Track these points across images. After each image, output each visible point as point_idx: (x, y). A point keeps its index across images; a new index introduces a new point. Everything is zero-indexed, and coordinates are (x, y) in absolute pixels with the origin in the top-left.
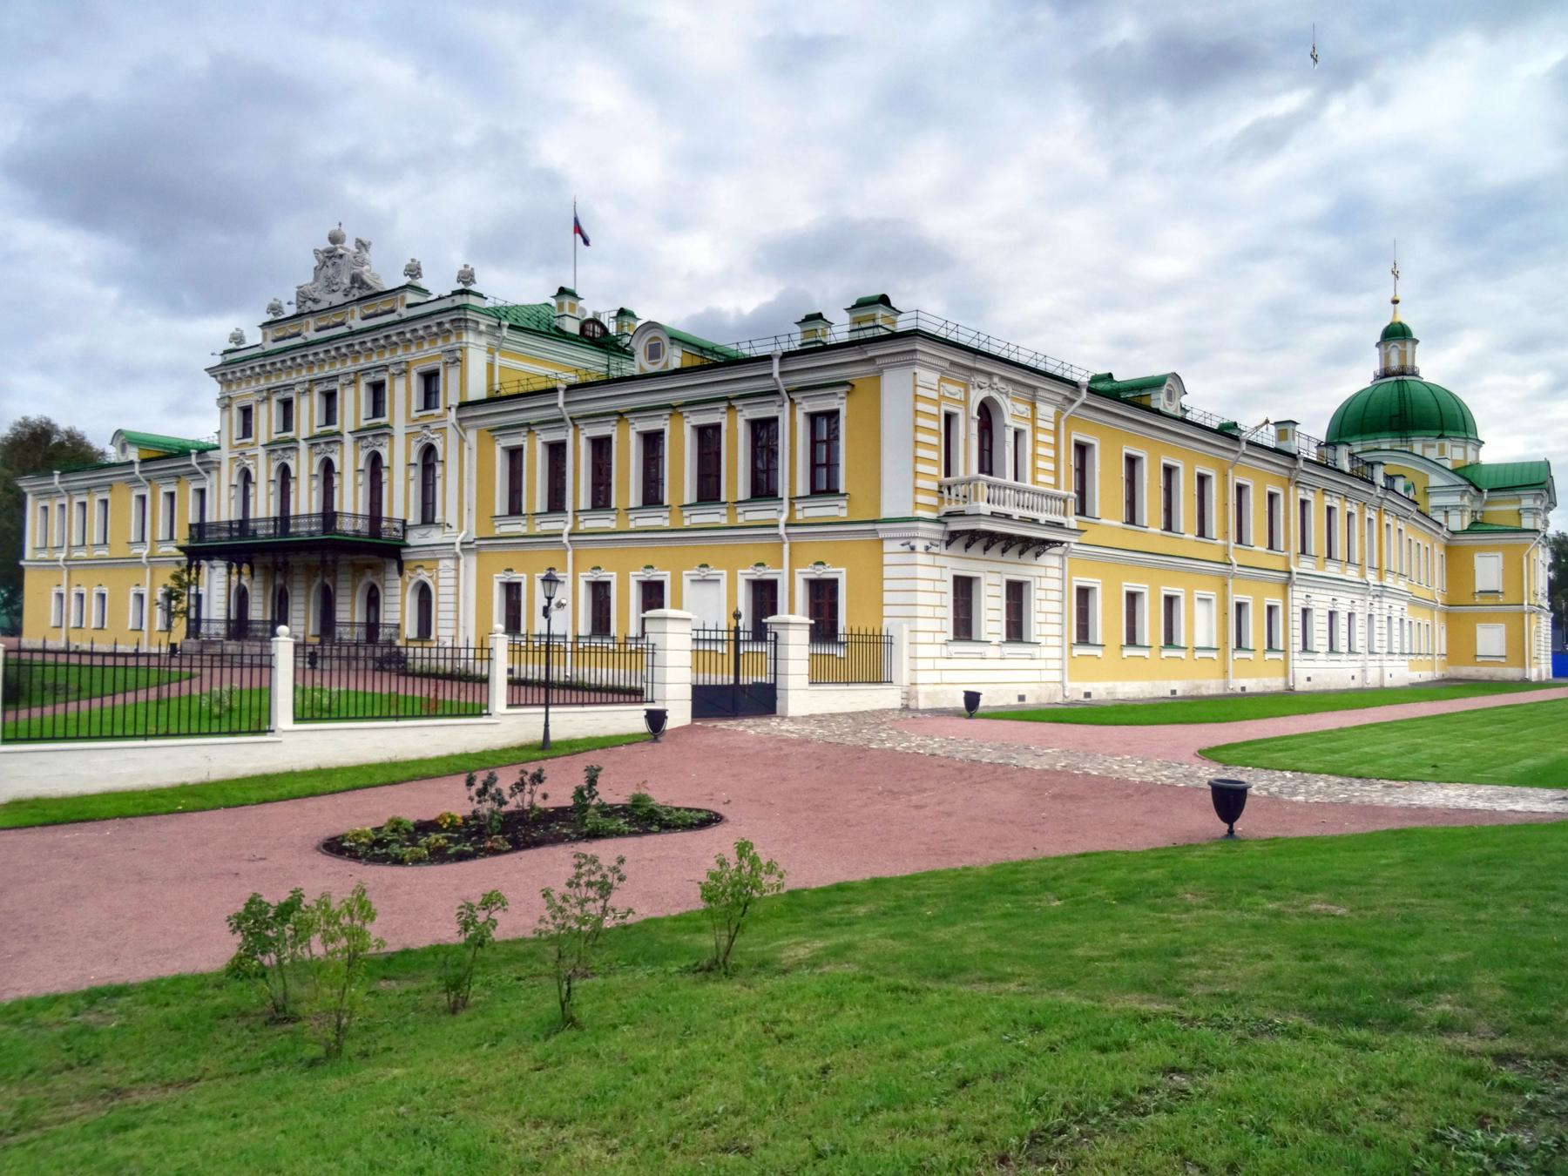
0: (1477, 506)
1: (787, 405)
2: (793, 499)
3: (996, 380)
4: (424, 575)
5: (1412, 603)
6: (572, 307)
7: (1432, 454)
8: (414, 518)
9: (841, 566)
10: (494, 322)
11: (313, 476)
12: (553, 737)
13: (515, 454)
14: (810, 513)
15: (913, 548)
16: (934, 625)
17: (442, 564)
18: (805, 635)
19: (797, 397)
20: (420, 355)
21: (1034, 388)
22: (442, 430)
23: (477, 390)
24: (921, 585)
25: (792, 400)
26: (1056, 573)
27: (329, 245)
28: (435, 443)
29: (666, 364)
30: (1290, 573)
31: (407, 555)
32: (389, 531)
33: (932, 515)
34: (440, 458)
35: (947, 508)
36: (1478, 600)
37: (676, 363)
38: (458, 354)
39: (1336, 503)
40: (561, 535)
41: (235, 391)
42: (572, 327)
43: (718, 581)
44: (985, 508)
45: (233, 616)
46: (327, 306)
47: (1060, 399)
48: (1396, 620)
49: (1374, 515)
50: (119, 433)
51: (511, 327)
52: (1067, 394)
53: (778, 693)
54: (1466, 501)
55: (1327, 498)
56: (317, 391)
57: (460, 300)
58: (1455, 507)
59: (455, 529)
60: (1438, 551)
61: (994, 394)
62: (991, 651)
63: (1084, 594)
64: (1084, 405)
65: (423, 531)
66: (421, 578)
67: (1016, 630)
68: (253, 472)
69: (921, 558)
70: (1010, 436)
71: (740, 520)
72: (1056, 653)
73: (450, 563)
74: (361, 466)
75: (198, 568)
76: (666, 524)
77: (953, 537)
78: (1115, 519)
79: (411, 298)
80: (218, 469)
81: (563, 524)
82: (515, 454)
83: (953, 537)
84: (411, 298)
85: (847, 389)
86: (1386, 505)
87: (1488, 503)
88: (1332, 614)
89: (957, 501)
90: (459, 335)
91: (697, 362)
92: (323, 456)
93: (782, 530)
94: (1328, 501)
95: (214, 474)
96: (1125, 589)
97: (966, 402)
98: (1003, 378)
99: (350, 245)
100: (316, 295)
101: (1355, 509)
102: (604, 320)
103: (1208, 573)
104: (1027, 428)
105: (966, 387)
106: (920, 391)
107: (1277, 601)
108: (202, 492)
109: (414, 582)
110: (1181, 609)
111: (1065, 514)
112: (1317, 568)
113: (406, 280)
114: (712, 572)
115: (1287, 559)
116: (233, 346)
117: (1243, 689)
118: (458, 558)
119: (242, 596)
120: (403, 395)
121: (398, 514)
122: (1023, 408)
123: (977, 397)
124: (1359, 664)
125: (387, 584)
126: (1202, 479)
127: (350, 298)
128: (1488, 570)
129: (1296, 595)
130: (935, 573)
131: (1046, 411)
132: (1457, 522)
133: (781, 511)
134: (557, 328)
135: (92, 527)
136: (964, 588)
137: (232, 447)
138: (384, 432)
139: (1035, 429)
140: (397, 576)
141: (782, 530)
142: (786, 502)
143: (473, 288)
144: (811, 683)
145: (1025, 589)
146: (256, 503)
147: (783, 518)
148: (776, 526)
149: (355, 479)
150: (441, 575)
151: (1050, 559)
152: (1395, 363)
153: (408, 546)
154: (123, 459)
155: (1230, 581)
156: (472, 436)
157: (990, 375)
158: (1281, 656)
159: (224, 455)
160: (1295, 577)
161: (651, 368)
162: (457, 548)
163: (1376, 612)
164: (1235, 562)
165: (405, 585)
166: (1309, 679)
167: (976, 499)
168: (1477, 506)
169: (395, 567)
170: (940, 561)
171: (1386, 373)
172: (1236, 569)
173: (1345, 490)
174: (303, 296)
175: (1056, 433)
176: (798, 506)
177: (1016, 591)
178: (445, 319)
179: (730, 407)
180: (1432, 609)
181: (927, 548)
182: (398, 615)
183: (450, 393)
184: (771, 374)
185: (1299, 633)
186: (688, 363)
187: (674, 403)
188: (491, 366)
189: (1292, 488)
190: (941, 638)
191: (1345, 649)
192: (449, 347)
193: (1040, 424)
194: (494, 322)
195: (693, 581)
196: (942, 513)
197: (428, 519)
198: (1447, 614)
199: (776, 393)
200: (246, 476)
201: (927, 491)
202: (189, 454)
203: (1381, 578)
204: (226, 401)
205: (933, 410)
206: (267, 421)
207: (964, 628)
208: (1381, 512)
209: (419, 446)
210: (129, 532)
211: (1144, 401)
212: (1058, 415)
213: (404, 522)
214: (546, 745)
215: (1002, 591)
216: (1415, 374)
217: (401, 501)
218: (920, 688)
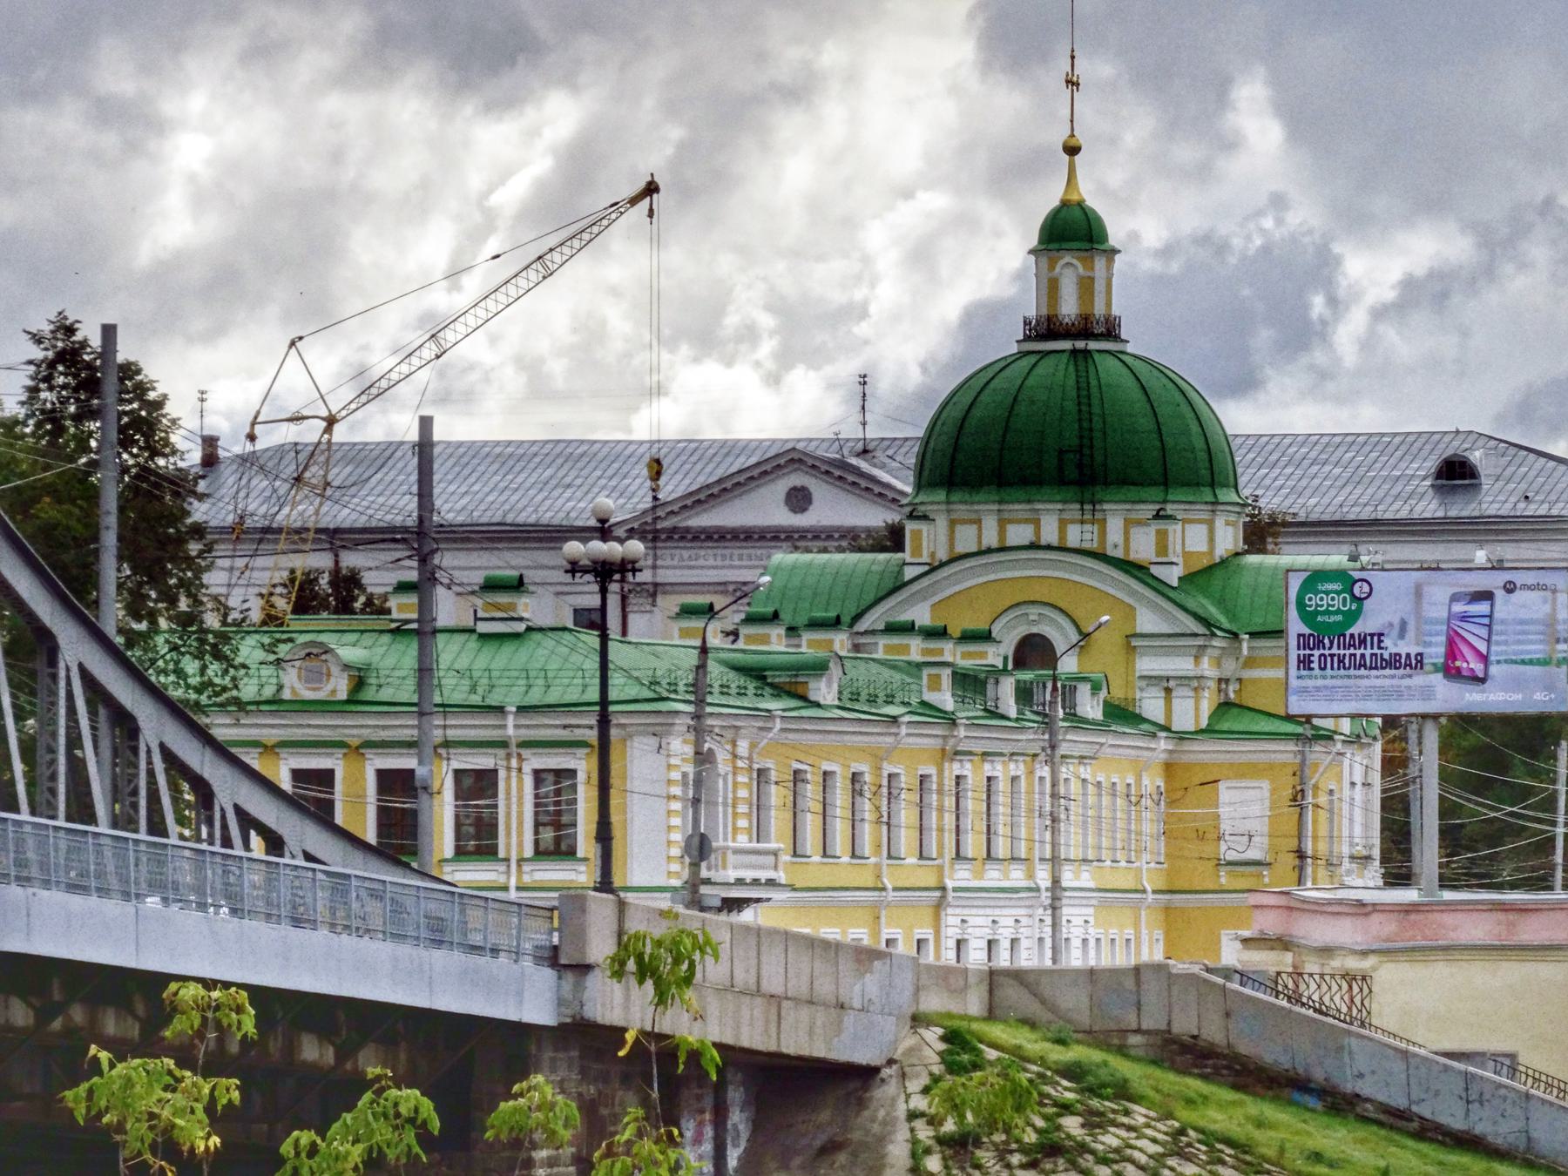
0: (1230, 667)
2: (521, 861)
7: (1143, 546)
14: (539, 876)
19: (525, 753)
25: (519, 755)
30: (944, 889)
54: (1207, 667)
58: (1184, 680)
87: (1250, 663)
103: (858, 904)
107: (927, 932)
115: (941, 868)
132: (1190, 712)
147: (513, 882)
148: (505, 889)
152: (1069, 308)
155: (884, 913)
160: (951, 894)
164: (889, 886)
168: (1230, 667)
171: (1046, 329)
176: (526, 868)
180: (1136, 907)
184: (504, 727)
198: (1167, 909)
216: (1111, 331)
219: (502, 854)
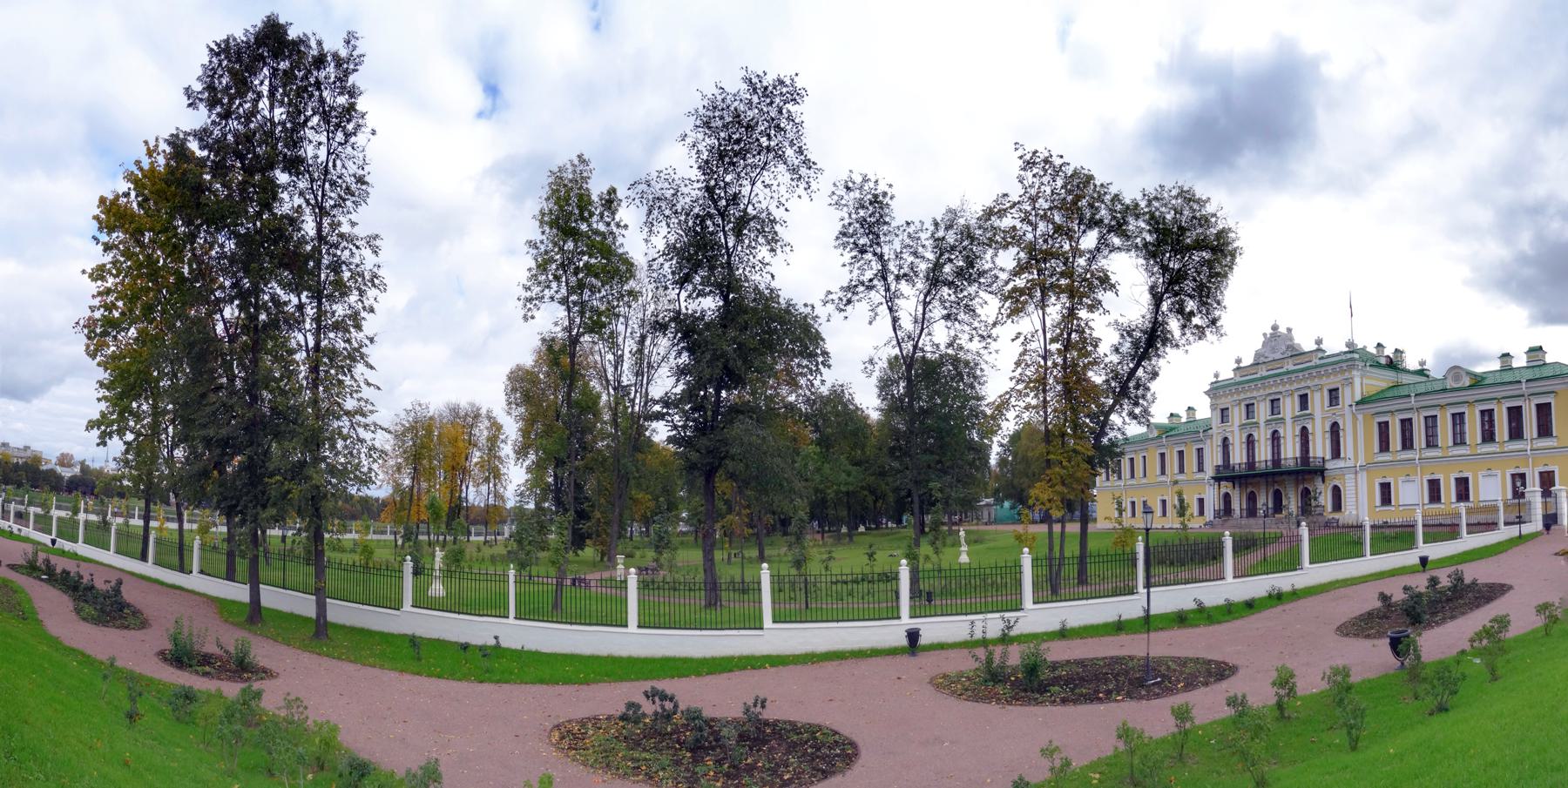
2: (1532, 439)
4: (1337, 483)
8: (1328, 456)
17: (1347, 477)
20: (1329, 381)
23: (1358, 397)
31: (1326, 473)
32: (1314, 464)
37: (1468, 384)
57: (1349, 356)
65: (1335, 461)
68: (1230, 438)
71: (1506, 449)
73: (1353, 476)
76: (1469, 452)
79: (1320, 355)
84: (1320, 355)
90: (1350, 372)
93: (1529, 452)
95: (1209, 441)
99: (1282, 330)
100: (1266, 355)
108: (1200, 451)
113: (1315, 347)
114: (1494, 472)
116: (1215, 380)
118: (1356, 473)
119: (1227, 497)
121: (1319, 454)
141: (1529, 452)
147: (1529, 448)
149: (1294, 439)
156: (1360, 417)
159: (1214, 431)
161: (1456, 386)
169: (1320, 479)
174: (1258, 355)
176: (1534, 442)
178: (1344, 365)
183: (1348, 397)
188: (1362, 384)
197: (1336, 453)
206: (1237, 416)
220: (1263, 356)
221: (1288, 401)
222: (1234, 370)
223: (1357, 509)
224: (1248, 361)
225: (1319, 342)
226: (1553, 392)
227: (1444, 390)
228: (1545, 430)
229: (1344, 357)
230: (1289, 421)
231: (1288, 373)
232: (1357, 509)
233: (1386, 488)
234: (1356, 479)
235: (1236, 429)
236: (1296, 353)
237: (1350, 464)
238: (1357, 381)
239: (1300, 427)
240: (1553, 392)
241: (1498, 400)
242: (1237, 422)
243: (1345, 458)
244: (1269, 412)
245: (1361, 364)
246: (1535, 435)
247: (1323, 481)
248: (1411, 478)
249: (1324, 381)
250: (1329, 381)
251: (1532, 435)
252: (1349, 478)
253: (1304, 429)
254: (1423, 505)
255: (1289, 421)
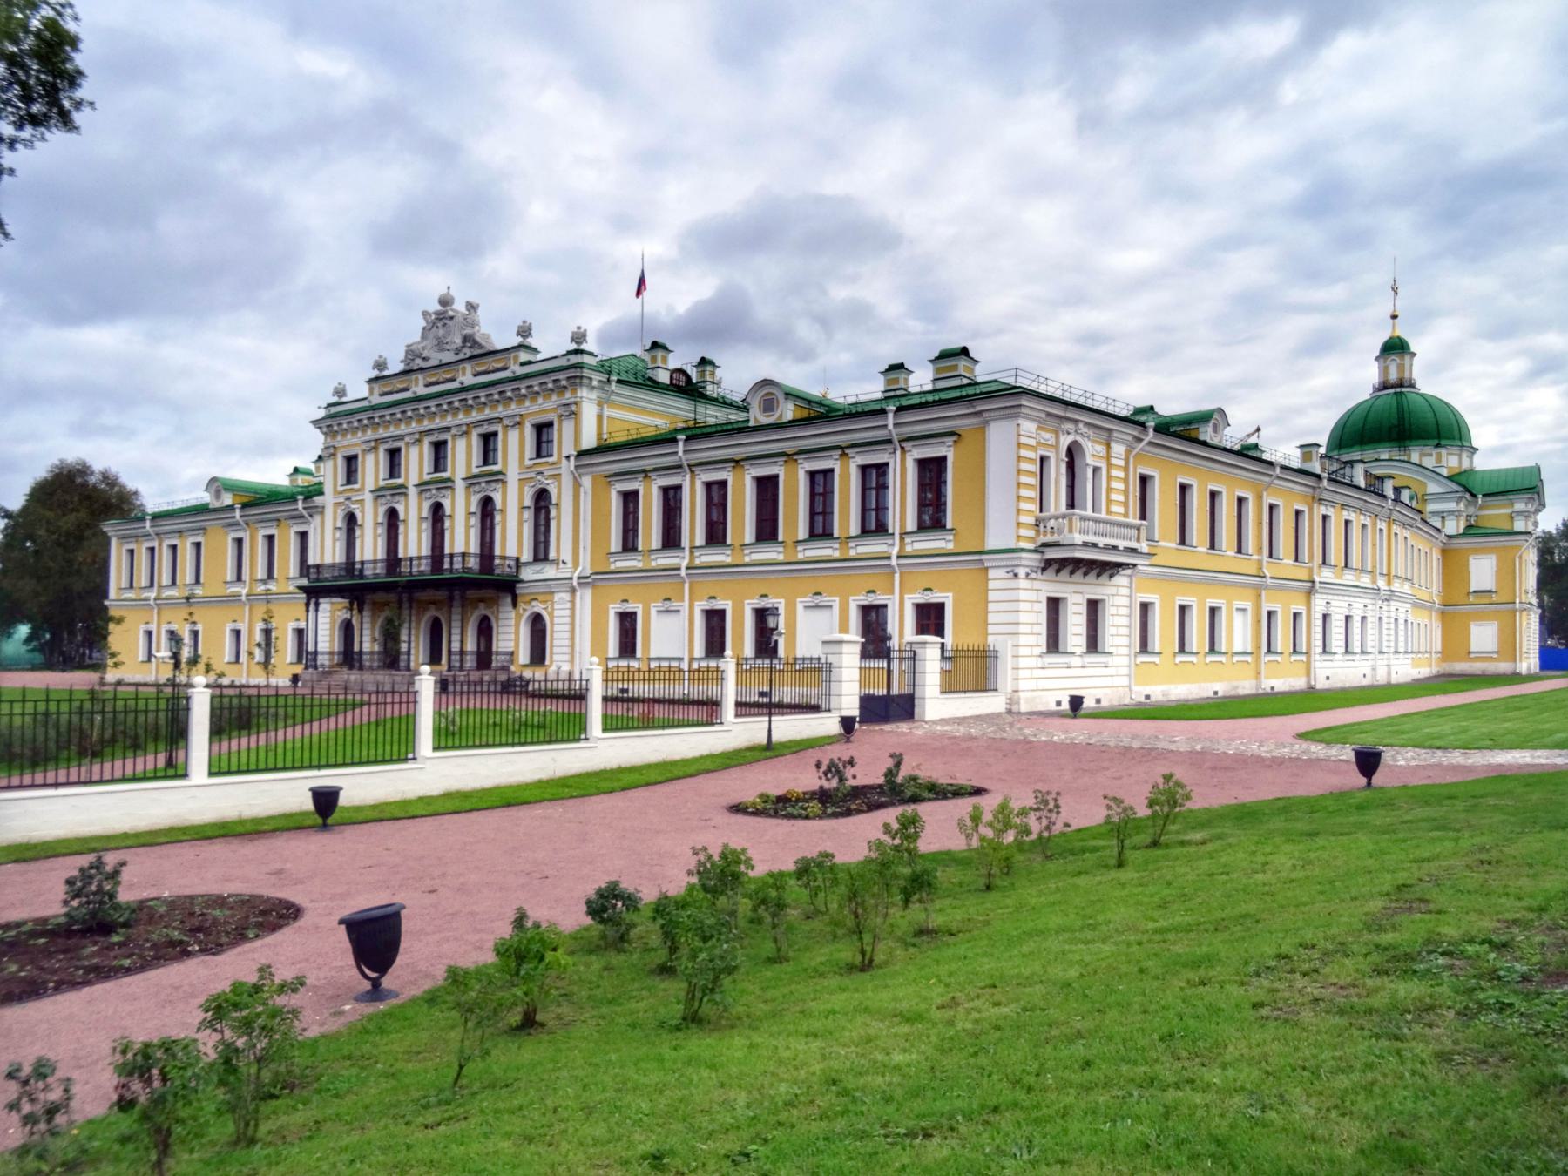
1: (898, 453)
2: (903, 535)
3: (1081, 425)
4: (538, 607)
5: (1415, 605)
6: (665, 360)
8: (526, 556)
9: (948, 591)
10: (604, 377)
11: (422, 519)
12: (775, 738)
13: (630, 498)
14: (918, 546)
15: (1016, 575)
16: (1032, 640)
17: (557, 597)
18: (857, 649)
19: (907, 445)
20: (535, 408)
21: (1110, 431)
22: (557, 477)
23: (589, 440)
24: (1023, 606)
25: (902, 448)
26: (1125, 591)
27: (439, 308)
28: (548, 488)
29: (781, 415)
30: (1313, 582)
31: (521, 589)
32: (502, 568)
33: (1031, 546)
34: (554, 501)
35: (1042, 539)
36: (1472, 599)
37: (789, 416)
38: (574, 408)
39: (1352, 516)
40: (679, 569)
41: (339, 441)
42: (663, 377)
43: (831, 607)
44: (1079, 538)
45: (482, 649)
46: (436, 363)
47: (1130, 438)
48: (1401, 621)
49: (1384, 525)
50: (214, 480)
51: (619, 381)
52: (1135, 433)
53: (916, 701)
55: (1345, 513)
56: (426, 441)
57: (574, 359)
59: (570, 565)
60: (1436, 555)
61: (1079, 438)
62: (1075, 661)
63: (1145, 607)
64: (1151, 443)
65: (538, 567)
66: (536, 609)
67: (1093, 644)
69: (1023, 583)
70: (1090, 472)
71: (852, 553)
72: (1125, 661)
73: (567, 596)
74: (473, 509)
75: (317, 605)
76: (781, 558)
77: (1048, 564)
78: (1170, 541)
79: (524, 356)
80: (322, 513)
81: (679, 559)
82: (630, 498)
83: (1048, 564)
84: (524, 356)
85: (955, 438)
86: (1395, 515)
88: (1347, 618)
89: (1045, 533)
90: (574, 392)
91: (805, 414)
92: (433, 501)
93: (894, 562)
94: (1346, 515)
95: (317, 518)
96: (1208, 605)
97: (1056, 447)
98: (1087, 424)
99: (459, 306)
101: (1368, 521)
102: (684, 368)
103: (1243, 585)
104: (1103, 466)
105: (1056, 433)
106: (1023, 440)
107: (1301, 608)
108: (303, 536)
109: (527, 614)
110: (1223, 618)
111: (1138, 540)
112: (1336, 577)
113: (517, 340)
114: (825, 600)
115: (1311, 570)
116: (335, 399)
117: (1272, 688)
118: (573, 591)
119: (347, 629)
120: (515, 448)
121: (512, 551)
122: (1100, 449)
123: (1065, 441)
124: (1370, 663)
125: (501, 616)
126: (1241, 501)
127: (461, 356)
128: (1482, 571)
129: (1318, 602)
130: (1032, 596)
131: (1118, 449)
132: (1453, 526)
133: (893, 545)
134: (650, 379)
135: (140, 564)
136: (1054, 605)
137: (336, 493)
138: (498, 478)
139: (1110, 466)
140: (510, 608)
141: (894, 562)
142: (897, 537)
143: (584, 347)
144: (943, 692)
145: (1100, 606)
146: (362, 542)
147: (895, 551)
148: (889, 558)
149: (467, 520)
150: (556, 606)
151: (1121, 580)
153: (522, 581)
154: (217, 504)
155: (1264, 593)
156: (587, 482)
157: (1076, 421)
158: (1303, 658)
159: (328, 500)
160: (1318, 585)
162: (575, 582)
163: (1384, 615)
165: (519, 617)
166: (1328, 678)
167: (1071, 531)
169: (509, 600)
170: (1037, 585)
172: (1269, 581)
173: (1360, 504)
174: (412, 354)
175: (1126, 469)
176: (908, 540)
177: (1094, 606)
178: (562, 376)
179: (844, 455)
180: (1430, 609)
181: (1027, 575)
182: (512, 644)
183: (565, 442)
184: (886, 426)
185: (1320, 636)
186: (798, 416)
187: (790, 451)
188: (600, 417)
189: (1315, 505)
190: (1037, 651)
191: (1358, 650)
192: (564, 401)
193: (1114, 461)
194: (604, 377)
195: (806, 607)
196: (1039, 544)
198: (1443, 613)
199: (889, 441)
200: (351, 519)
201: (1027, 525)
202: (296, 500)
203: (1389, 583)
204: (332, 451)
205: (1031, 455)
206: (373, 470)
207: (1054, 644)
208: (1390, 521)
209: (532, 491)
210: (226, 574)
211: (1193, 434)
212: (1128, 453)
213: (517, 559)
214: (769, 746)
215: (1083, 609)
217: (513, 539)
218: (1021, 694)
219: (890, 531)
220: (419, 356)
221: (461, 444)
222: (371, 381)
223: (572, 661)
224: (395, 366)
225: (525, 331)
226: (952, 434)
227: (741, 429)
228: (932, 516)
229: (563, 362)
230: (460, 485)
231: (464, 389)
232: (572, 661)
233: (627, 622)
234: (573, 602)
235: (368, 497)
236: (479, 353)
237: (564, 572)
238: (589, 412)
239: (479, 496)
240: (952, 434)
241: (843, 451)
242: (370, 484)
243: (556, 562)
244: (428, 465)
245: (597, 378)
246: (911, 525)
247: (515, 605)
248: (674, 605)
249: (528, 407)
250: (535, 408)
251: (903, 524)
252: (562, 598)
253: (487, 503)
254: (692, 659)
255: (460, 485)
